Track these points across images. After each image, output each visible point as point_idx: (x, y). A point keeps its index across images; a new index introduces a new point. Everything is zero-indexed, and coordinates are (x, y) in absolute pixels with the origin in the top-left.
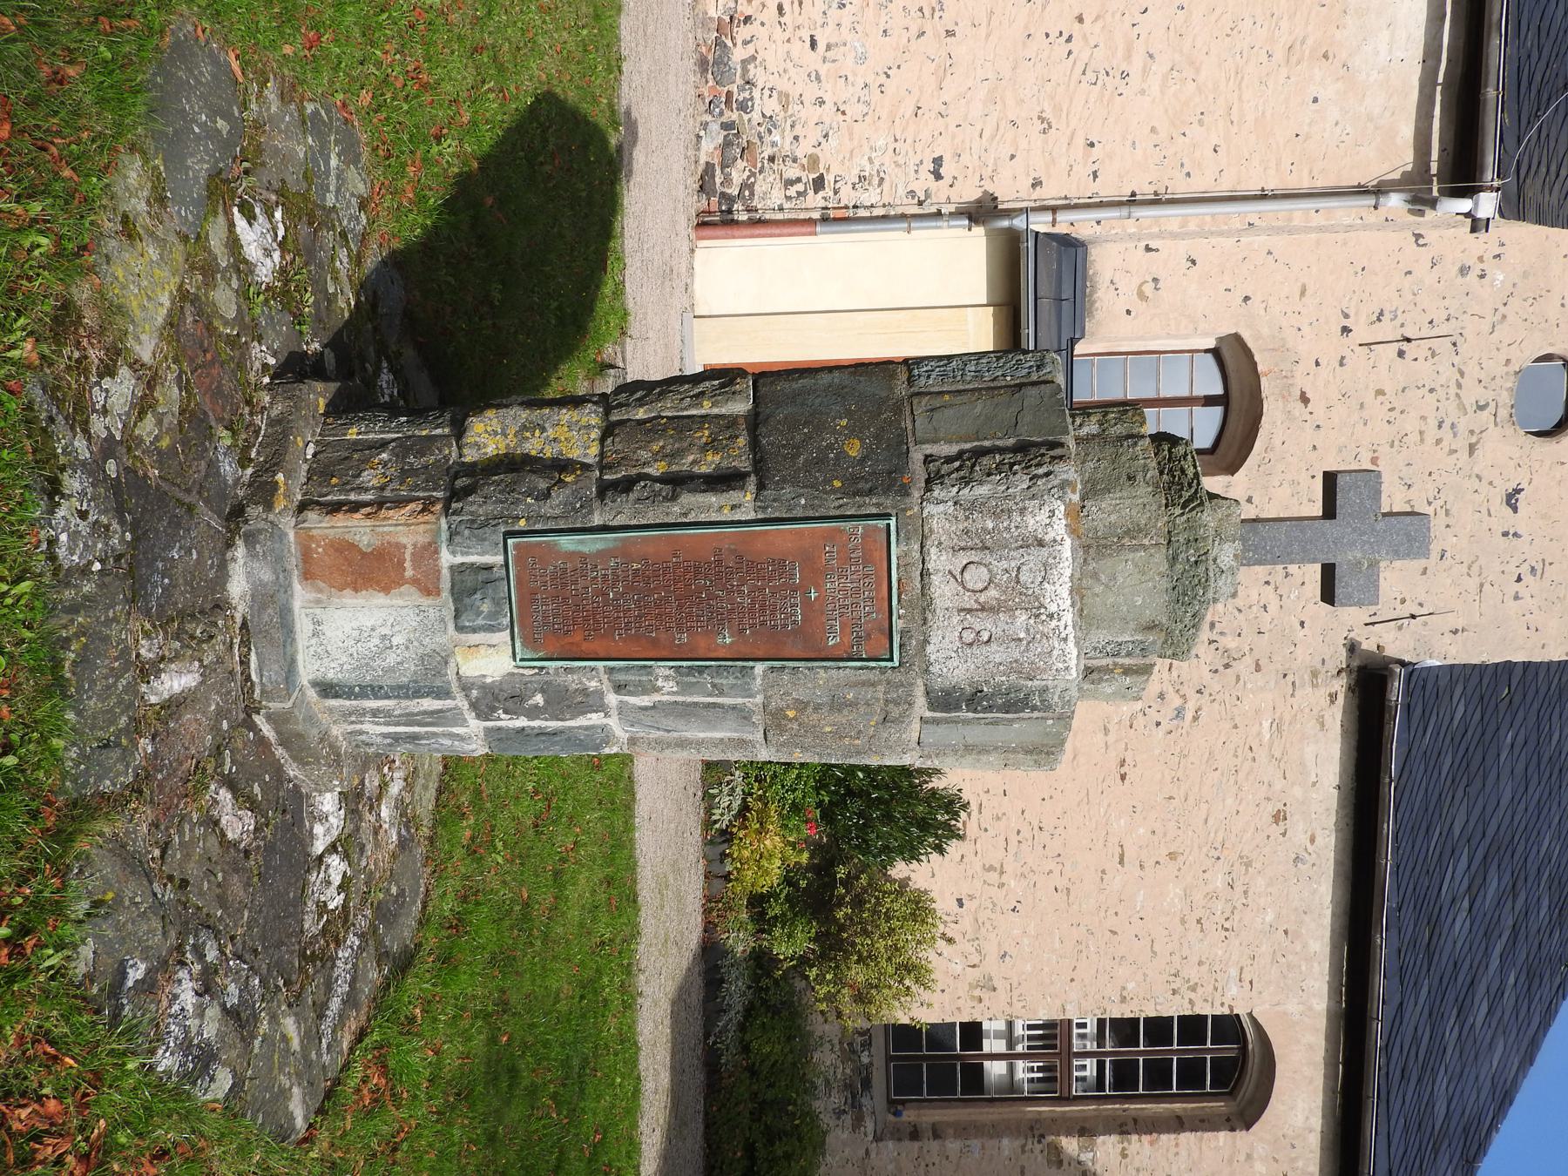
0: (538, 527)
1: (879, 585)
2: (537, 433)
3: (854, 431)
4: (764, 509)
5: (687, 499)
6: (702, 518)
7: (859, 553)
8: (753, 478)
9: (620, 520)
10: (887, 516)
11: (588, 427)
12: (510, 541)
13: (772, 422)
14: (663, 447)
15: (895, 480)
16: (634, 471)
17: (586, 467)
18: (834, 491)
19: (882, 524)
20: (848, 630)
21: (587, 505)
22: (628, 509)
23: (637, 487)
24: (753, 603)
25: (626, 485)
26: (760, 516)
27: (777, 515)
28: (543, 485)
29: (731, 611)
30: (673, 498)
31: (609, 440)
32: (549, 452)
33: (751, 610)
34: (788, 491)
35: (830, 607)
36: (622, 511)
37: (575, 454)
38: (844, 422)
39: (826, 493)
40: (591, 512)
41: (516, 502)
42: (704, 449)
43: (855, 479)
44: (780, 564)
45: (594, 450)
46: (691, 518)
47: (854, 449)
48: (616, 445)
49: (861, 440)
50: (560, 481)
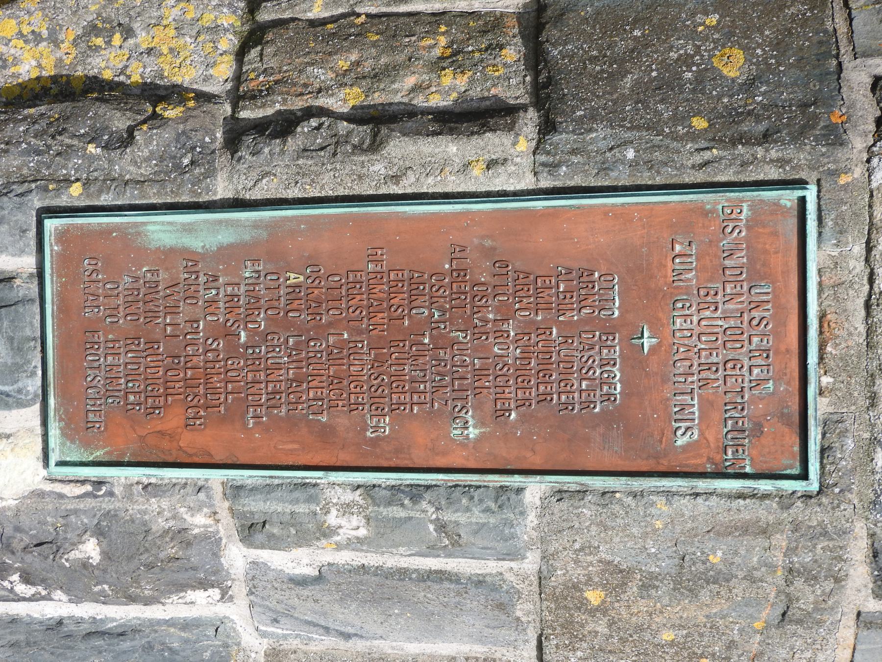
0: (105, 199)
1: (781, 323)
2: (117, 39)
3: (728, 36)
4: (552, 167)
5: (400, 148)
6: (429, 185)
7: (741, 258)
8: (532, 114)
9: (266, 189)
10: (801, 183)
11: (215, 29)
12: (50, 224)
13: (571, 19)
14: (358, 63)
15: (816, 117)
16: (298, 104)
17: (204, 97)
18: (693, 136)
19: (788, 197)
20: (716, 416)
21: (203, 161)
22: (283, 167)
23: (304, 128)
24: (526, 356)
25: (283, 126)
26: (546, 183)
27: (577, 181)
28: (120, 122)
29: (480, 374)
30: (375, 146)
31: (254, 53)
32: (137, 74)
33: (521, 372)
34: (600, 136)
35: (682, 367)
36: (272, 171)
37: (187, 77)
38: (713, 20)
39: (676, 138)
40: (211, 173)
41: (65, 153)
42: (438, 66)
43: (734, 116)
44: (582, 278)
45: (225, 69)
46: (406, 186)
47: (733, 65)
48: (265, 60)
49: (745, 48)
50: (155, 116)
